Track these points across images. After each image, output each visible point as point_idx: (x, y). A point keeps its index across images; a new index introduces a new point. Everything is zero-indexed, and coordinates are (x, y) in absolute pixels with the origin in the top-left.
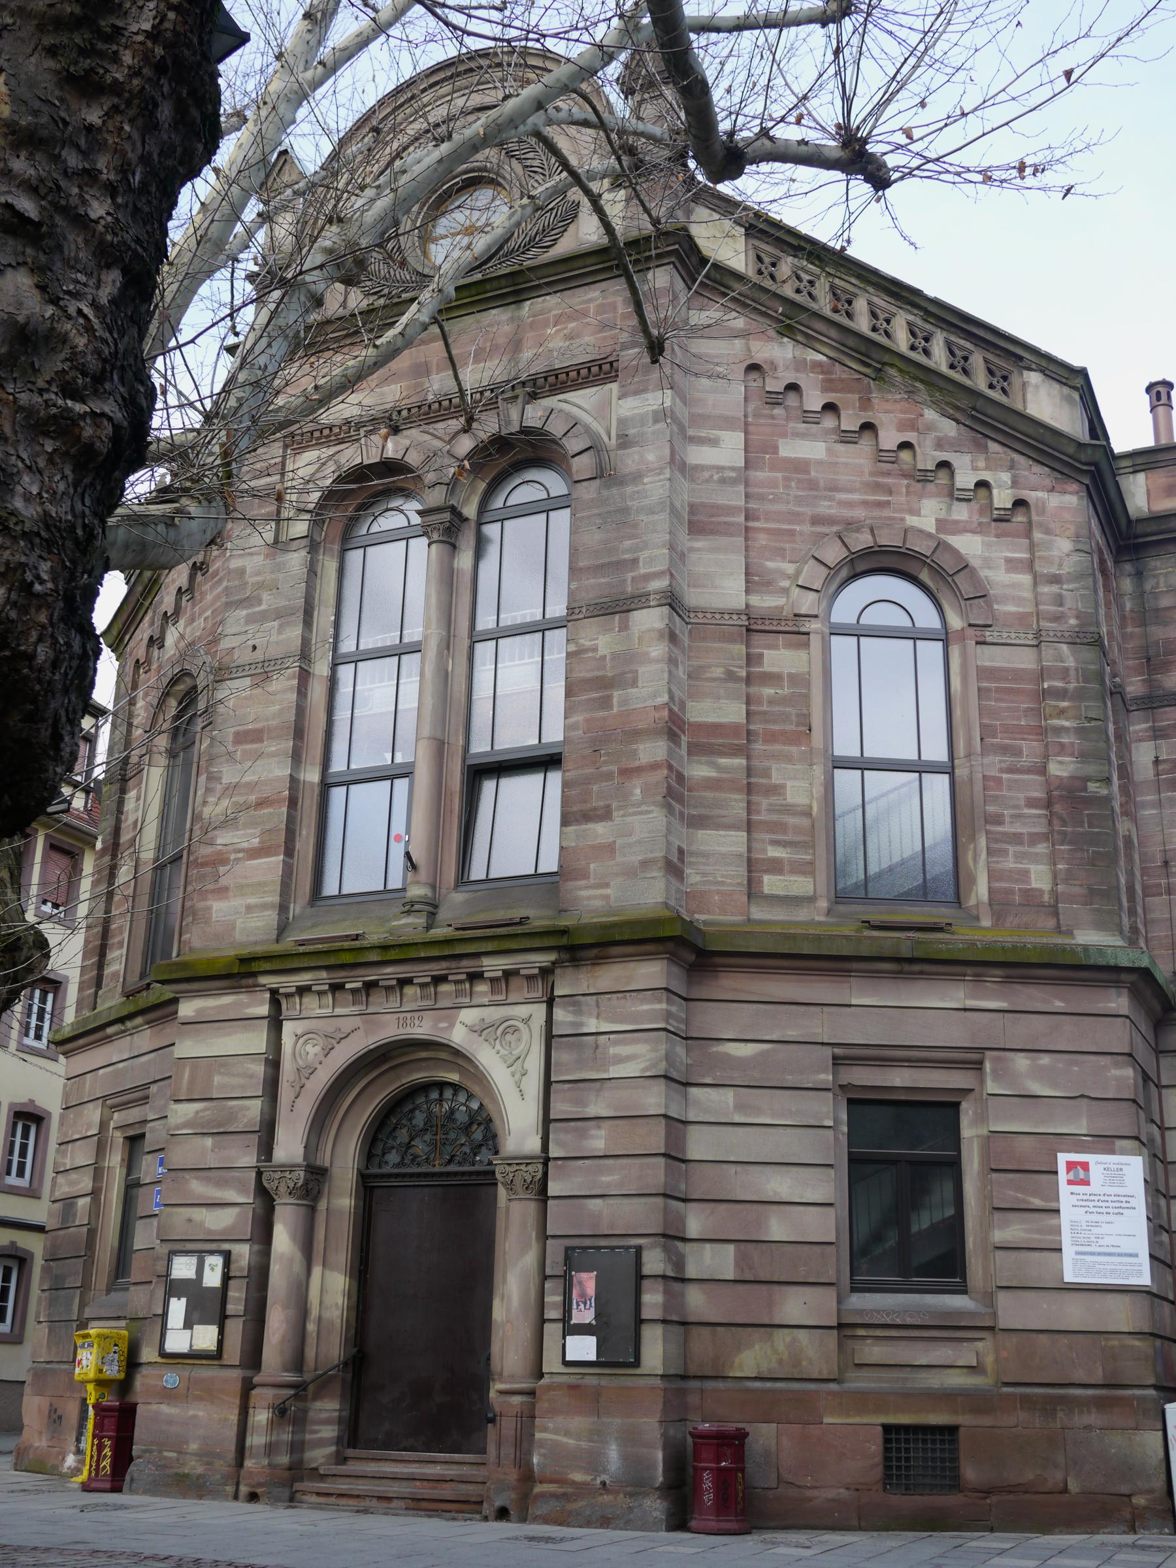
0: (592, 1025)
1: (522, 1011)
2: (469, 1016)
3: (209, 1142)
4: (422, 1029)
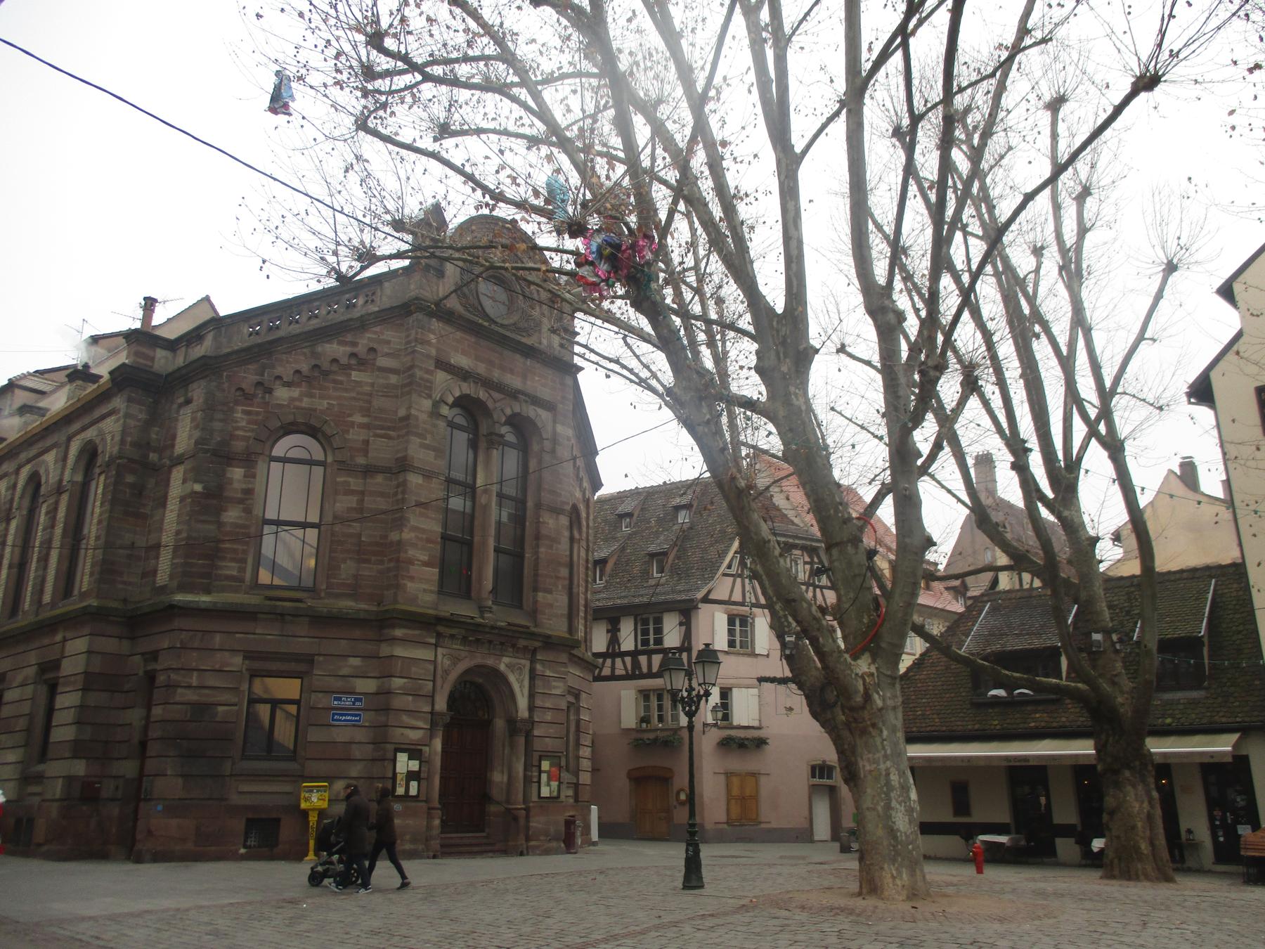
0: (548, 673)
1: (523, 661)
2: (506, 660)
3: (410, 698)
4: (490, 662)
